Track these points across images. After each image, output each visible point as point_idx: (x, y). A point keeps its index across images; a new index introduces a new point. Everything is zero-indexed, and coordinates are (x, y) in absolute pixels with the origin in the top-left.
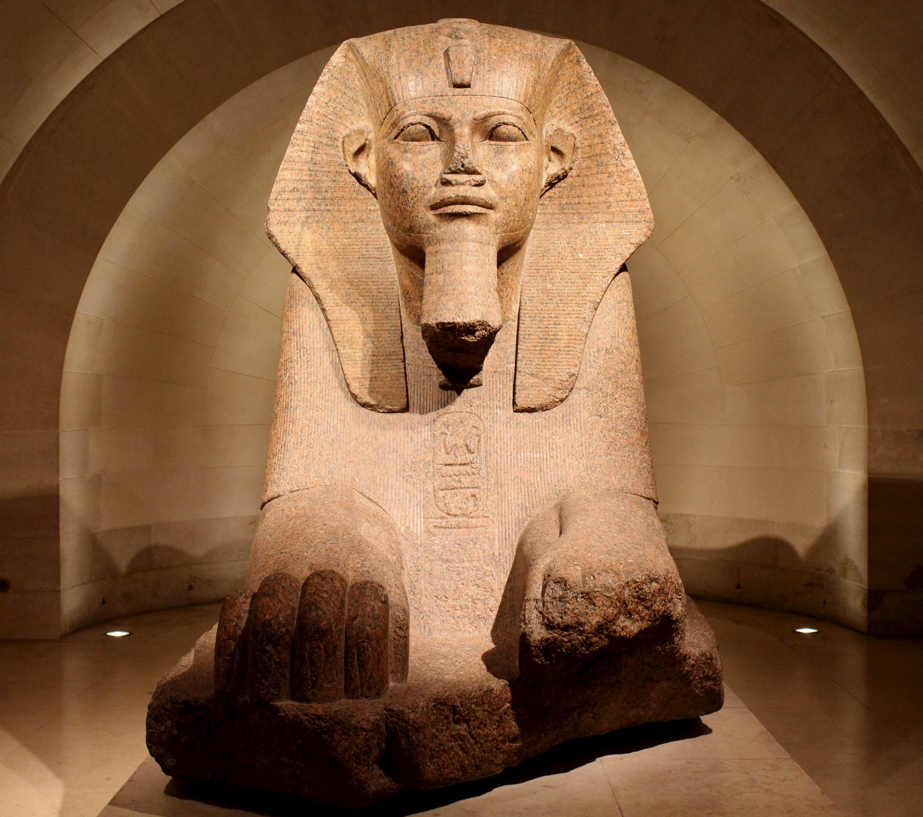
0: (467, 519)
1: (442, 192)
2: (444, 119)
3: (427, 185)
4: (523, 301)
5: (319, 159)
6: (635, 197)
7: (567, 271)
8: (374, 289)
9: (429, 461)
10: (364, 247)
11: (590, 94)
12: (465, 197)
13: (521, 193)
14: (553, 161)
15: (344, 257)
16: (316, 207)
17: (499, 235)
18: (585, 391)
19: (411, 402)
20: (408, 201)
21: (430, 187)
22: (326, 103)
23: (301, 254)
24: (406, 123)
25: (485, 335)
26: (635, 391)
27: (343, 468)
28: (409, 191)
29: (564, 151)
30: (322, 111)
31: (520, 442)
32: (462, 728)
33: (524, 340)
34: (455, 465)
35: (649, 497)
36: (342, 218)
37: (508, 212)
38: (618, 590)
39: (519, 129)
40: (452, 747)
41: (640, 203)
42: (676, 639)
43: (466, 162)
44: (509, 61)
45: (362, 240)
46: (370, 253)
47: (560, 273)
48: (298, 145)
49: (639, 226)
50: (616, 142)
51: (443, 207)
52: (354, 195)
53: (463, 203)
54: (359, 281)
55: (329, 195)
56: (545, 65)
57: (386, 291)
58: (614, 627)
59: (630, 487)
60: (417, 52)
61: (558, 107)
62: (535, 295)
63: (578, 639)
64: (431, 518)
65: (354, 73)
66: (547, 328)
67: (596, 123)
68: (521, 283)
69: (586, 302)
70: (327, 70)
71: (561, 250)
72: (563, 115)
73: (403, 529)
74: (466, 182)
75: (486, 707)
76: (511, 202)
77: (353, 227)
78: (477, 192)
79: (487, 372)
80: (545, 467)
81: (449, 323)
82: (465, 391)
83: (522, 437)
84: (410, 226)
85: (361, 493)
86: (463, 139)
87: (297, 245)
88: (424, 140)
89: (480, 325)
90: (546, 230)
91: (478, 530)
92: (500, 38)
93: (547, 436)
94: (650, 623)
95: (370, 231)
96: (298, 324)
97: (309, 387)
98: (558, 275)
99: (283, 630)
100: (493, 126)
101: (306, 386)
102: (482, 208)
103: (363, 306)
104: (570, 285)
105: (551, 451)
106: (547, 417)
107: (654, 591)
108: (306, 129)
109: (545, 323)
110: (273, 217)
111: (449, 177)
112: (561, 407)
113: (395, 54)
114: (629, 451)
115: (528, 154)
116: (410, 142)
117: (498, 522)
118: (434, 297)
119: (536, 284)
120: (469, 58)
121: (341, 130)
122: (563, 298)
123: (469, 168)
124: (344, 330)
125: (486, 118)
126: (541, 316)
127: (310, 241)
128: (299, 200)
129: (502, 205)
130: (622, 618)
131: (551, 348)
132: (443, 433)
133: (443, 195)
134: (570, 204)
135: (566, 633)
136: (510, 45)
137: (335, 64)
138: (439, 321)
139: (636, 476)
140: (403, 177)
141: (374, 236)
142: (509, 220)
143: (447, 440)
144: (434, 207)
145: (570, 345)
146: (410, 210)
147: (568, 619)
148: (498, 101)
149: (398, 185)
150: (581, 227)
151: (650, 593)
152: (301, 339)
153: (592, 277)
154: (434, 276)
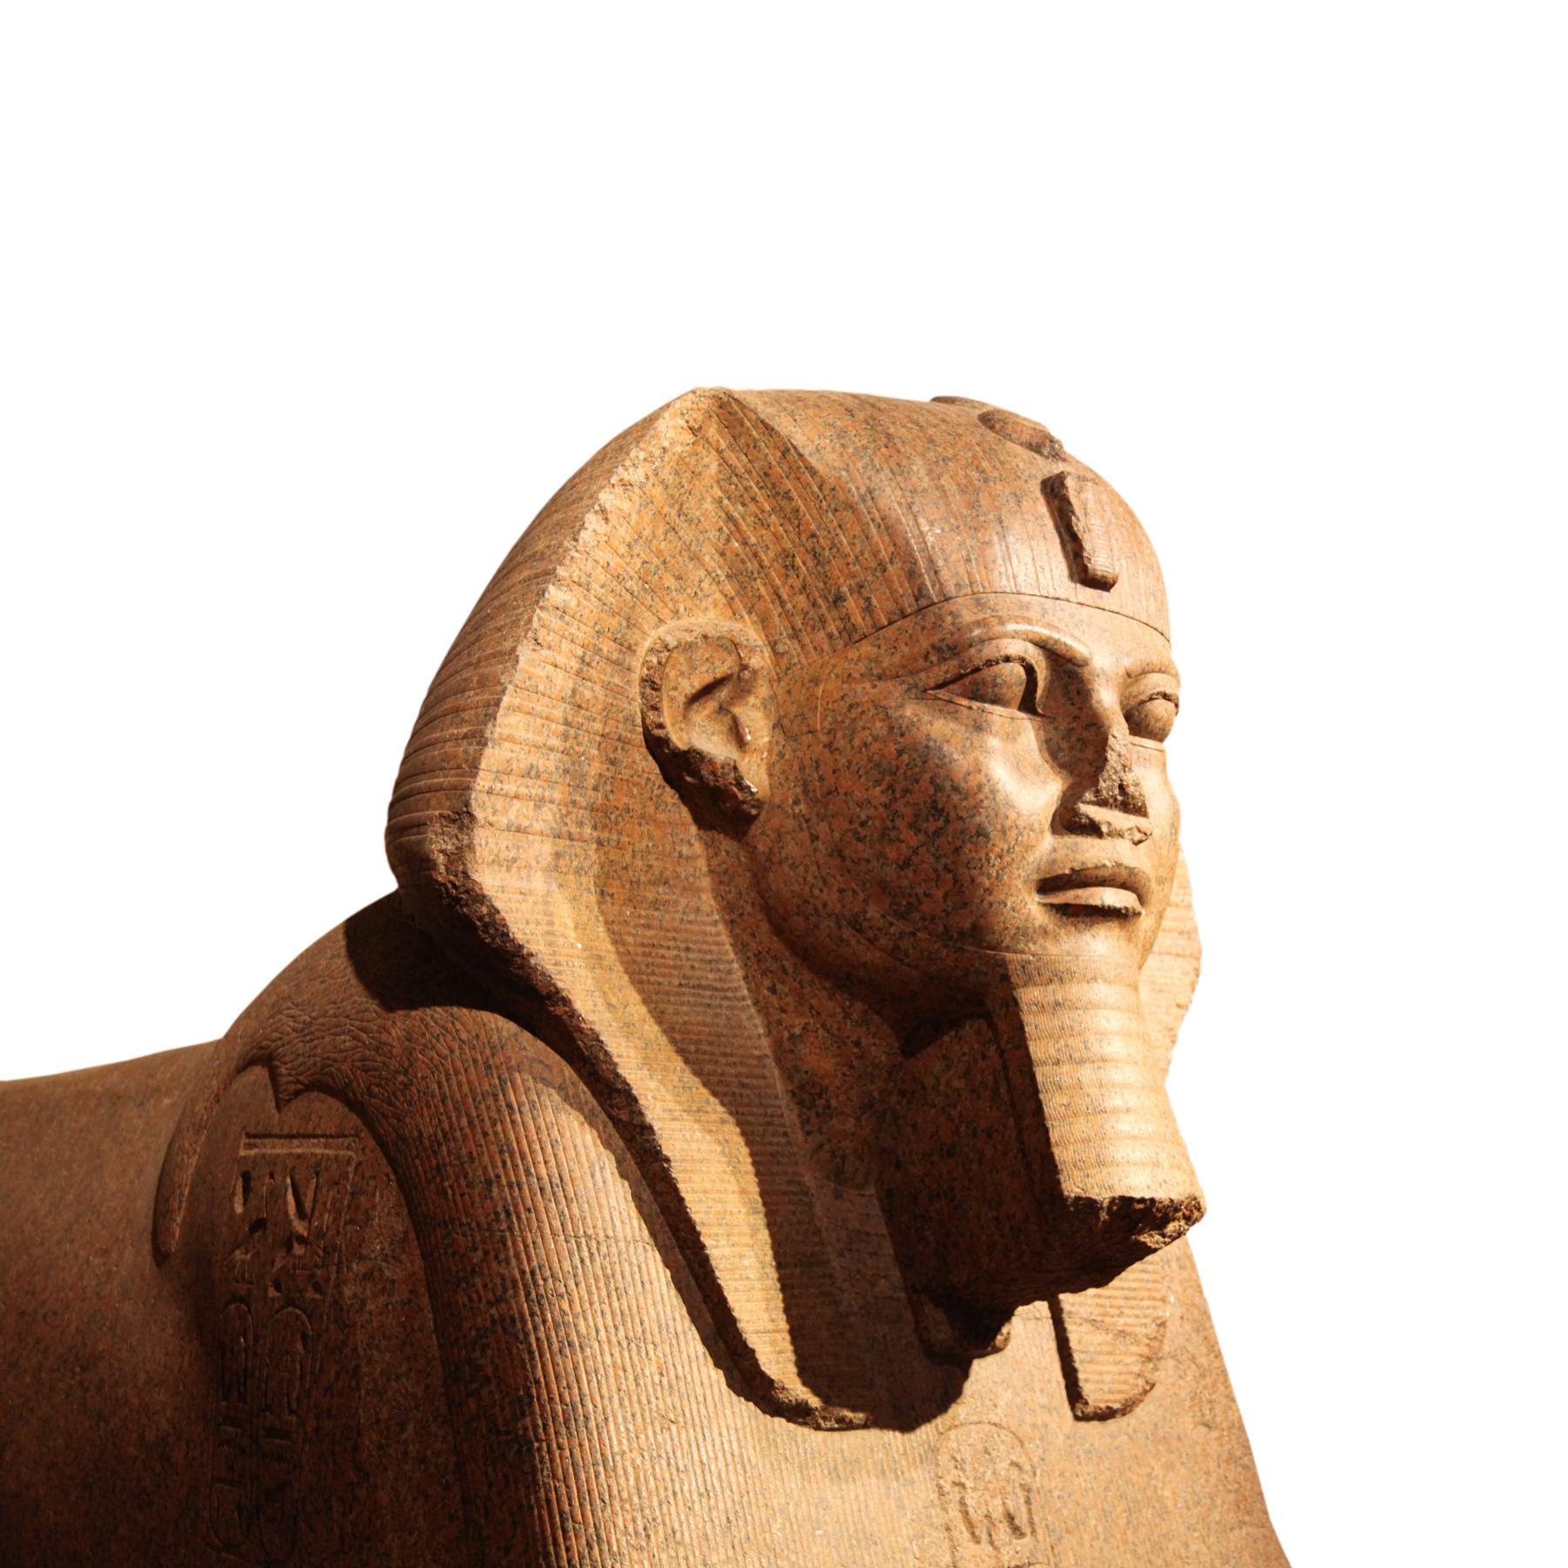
1: (1076, 847)
3: (1036, 826)
5: (588, 694)
8: (731, 1075)
10: (683, 954)
12: (1131, 871)
15: (652, 979)
16: (574, 830)
20: (988, 860)
21: (1042, 832)
23: (562, 959)
24: (989, 651)
36: (626, 868)
43: (1129, 778)
45: (674, 934)
46: (698, 973)
48: (550, 648)
52: (651, 810)
53: (1124, 886)
54: (696, 1052)
57: (755, 1082)
65: (707, 481)
70: (642, 455)
77: (650, 896)
84: (974, 927)
87: (548, 933)
95: (684, 913)
96: (553, 1162)
97: (626, 1354)
100: (1144, 697)
101: (616, 1351)
103: (723, 1122)
106: (1130, 1430)
108: (573, 604)
116: (987, 706)
118: (1081, 1127)
121: (645, 627)
123: (1133, 798)
127: (571, 924)
128: (540, 802)
132: (955, 1484)
133: (1080, 857)
137: (666, 444)
138: (1116, 1194)
140: (981, 796)
141: (695, 928)
143: (969, 1501)
144: (1047, 885)
146: (987, 883)
149: (965, 815)
152: (576, 1211)
154: (1065, 1068)
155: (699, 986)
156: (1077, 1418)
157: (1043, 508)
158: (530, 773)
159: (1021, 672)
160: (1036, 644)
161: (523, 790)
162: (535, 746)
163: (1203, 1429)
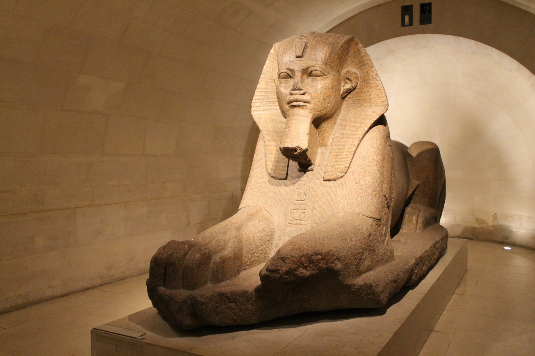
0: (300, 221)
1: (290, 98)
2: (292, 70)
3: (286, 95)
4: (333, 138)
6: (380, 96)
7: (352, 126)
9: (291, 199)
11: (362, 56)
12: (296, 99)
13: (321, 97)
14: (348, 83)
16: (267, 105)
17: (313, 113)
18: (352, 173)
19: (288, 176)
21: (287, 96)
22: (270, 67)
25: (300, 152)
26: (373, 174)
27: (262, 200)
28: (280, 98)
29: (352, 79)
30: (269, 70)
31: (324, 193)
32: (233, 305)
33: (331, 153)
34: (300, 200)
35: (371, 217)
37: (315, 104)
38: (298, 258)
39: (321, 72)
40: (227, 312)
41: (382, 98)
42: (340, 278)
43: (298, 86)
44: (319, 46)
47: (348, 127)
49: (382, 107)
50: (373, 74)
51: (292, 102)
53: (296, 102)
55: (272, 100)
56: (337, 46)
58: (296, 272)
59: (363, 212)
60: (288, 46)
61: (351, 62)
62: (338, 136)
63: (277, 276)
64: (288, 220)
66: (340, 148)
67: (365, 67)
68: (334, 131)
69: (356, 138)
71: (351, 118)
72: (353, 65)
73: (277, 224)
74: (298, 93)
75: (245, 298)
76: (316, 100)
78: (302, 97)
79: (317, 165)
80: (331, 202)
81: (286, 147)
82: (307, 172)
83: (325, 190)
85: (265, 210)
86: (297, 77)
88: (287, 78)
89: (298, 148)
90: (348, 110)
91: (304, 226)
92: (318, 38)
93: (335, 191)
94: (318, 272)
98: (348, 127)
99: (162, 262)
100: (310, 71)
102: (305, 103)
103: (278, 140)
104: (351, 131)
105: (335, 197)
107: (318, 259)
109: (340, 146)
110: (253, 109)
111: (292, 92)
112: (341, 179)
113: (281, 47)
114: (366, 198)
115: (326, 81)
116: (282, 80)
117: (311, 223)
119: (339, 131)
120: (302, 46)
122: (348, 137)
124: (270, 149)
125: (307, 68)
126: (339, 144)
128: (261, 102)
129: (313, 101)
130: (301, 269)
131: (340, 156)
134: (357, 99)
135: (272, 273)
136: (321, 40)
139: (367, 208)
142: (316, 107)
143: (298, 191)
145: (347, 155)
147: (273, 268)
148: (312, 61)
150: (360, 109)
151: (316, 259)
153: (360, 128)
155: (283, 122)
156: (324, 181)
157: (294, 48)
158: (260, 99)
159: (286, 74)
160: (287, 69)
161: (259, 101)
162: (261, 95)
163: (355, 184)
